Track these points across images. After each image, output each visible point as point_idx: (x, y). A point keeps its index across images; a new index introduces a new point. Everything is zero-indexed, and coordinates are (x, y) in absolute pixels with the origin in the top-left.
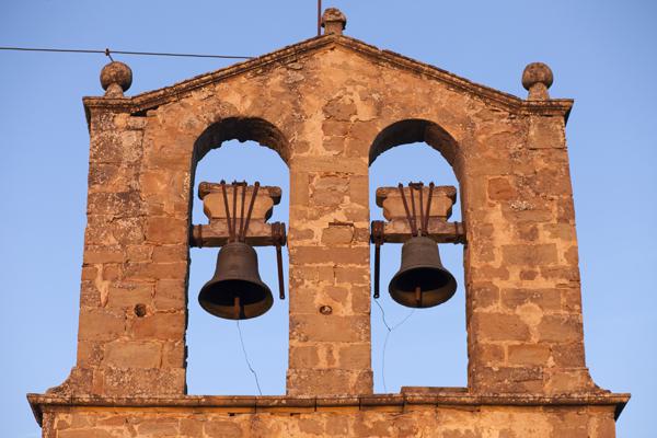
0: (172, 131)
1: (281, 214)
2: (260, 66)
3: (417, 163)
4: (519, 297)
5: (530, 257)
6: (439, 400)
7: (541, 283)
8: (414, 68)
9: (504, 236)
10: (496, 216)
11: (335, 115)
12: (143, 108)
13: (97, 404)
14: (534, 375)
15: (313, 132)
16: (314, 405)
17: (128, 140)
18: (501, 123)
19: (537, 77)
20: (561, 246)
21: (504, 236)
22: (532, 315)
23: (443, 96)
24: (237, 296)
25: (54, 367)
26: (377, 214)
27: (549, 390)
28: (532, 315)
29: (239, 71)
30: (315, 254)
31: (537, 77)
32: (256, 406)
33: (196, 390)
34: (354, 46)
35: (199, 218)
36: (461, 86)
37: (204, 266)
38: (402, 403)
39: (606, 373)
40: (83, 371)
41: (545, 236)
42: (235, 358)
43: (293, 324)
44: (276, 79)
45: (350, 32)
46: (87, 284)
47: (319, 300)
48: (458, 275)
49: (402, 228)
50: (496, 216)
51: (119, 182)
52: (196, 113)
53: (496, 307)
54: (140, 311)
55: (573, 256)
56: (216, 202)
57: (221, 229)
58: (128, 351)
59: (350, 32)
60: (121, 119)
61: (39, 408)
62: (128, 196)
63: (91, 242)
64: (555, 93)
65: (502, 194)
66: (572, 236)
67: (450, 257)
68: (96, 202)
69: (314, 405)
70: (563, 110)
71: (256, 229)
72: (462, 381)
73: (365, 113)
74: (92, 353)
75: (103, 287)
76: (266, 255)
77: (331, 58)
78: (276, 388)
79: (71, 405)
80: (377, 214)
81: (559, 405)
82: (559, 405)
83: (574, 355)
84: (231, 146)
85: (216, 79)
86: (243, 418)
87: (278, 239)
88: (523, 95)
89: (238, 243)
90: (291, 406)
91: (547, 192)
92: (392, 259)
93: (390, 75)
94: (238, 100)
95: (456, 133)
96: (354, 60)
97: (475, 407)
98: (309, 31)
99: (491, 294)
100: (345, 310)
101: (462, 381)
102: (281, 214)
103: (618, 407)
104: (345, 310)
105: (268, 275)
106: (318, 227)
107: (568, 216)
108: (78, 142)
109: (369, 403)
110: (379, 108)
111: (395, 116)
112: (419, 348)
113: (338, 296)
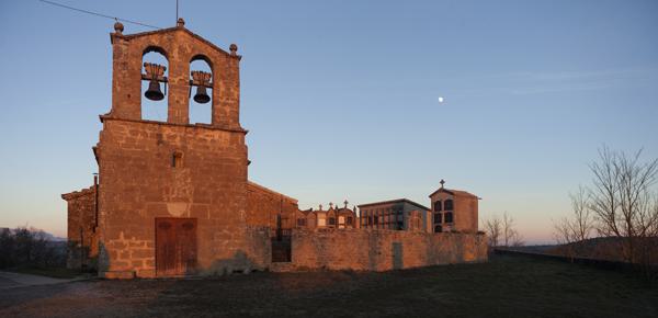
0: (137, 47)
1: (166, 74)
2: (162, 32)
3: (200, 66)
4: (225, 104)
5: (228, 95)
6: (204, 127)
8: (203, 41)
9: (222, 89)
10: (221, 83)
12: (128, 38)
13: (119, 119)
15: (175, 54)
17: (124, 48)
18: (224, 59)
19: (234, 48)
20: (236, 93)
21: (222, 89)
22: (228, 109)
24: (154, 95)
25: (107, 109)
26: (191, 78)
27: (231, 127)
28: (228, 109)
29: (155, 33)
30: (175, 87)
31: (234, 48)
32: (160, 124)
33: (144, 118)
34: (187, 31)
35: (144, 72)
36: (215, 48)
37: (145, 86)
38: (196, 127)
39: (243, 124)
42: (155, 111)
43: (169, 104)
44: (165, 37)
46: (114, 87)
48: (210, 96)
49: (197, 82)
50: (221, 83)
51: (122, 59)
53: (219, 106)
54: (129, 96)
55: (238, 96)
56: (149, 68)
57: (150, 76)
58: (125, 105)
60: (122, 41)
61: (102, 119)
62: (124, 64)
63: (114, 76)
64: (238, 53)
65: (223, 78)
66: (238, 91)
67: (209, 92)
68: (116, 64)
69: (175, 125)
70: (239, 58)
71: (159, 78)
72: (210, 123)
73: (189, 51)
75: (118, 88)
76: (162, 84)
78: (164, 119)
79: (112, 119)
80: (191, 78)
81: (233, 131)
82: (233, 131)
83: (237, 120)
84: (152, 53)
85: (149, 34)
86: (157, 126)
87: (165, 81)
88: (229, 52)
89: (155, 81)
90: (168, 125)
91: (233, 79)
92: (194, 90)
93: (196, 41)
94: (155, 41)
95: (212, 60)
96: (187, 35)
97: (213, 129)
98: (174, 25)
99: (218, 103)
100: (182, 102)
101: (210, 123)
102: (166, 74)
103: (246, 133)
104: (182, 102)
105: (163, 91)
106: (176, 80)
107: (238, 86)
108: (108, 49)
109: (188, 126)
110: (193, 50)
111: (197, 53)
112: (200, 114)
113: (181, 98)
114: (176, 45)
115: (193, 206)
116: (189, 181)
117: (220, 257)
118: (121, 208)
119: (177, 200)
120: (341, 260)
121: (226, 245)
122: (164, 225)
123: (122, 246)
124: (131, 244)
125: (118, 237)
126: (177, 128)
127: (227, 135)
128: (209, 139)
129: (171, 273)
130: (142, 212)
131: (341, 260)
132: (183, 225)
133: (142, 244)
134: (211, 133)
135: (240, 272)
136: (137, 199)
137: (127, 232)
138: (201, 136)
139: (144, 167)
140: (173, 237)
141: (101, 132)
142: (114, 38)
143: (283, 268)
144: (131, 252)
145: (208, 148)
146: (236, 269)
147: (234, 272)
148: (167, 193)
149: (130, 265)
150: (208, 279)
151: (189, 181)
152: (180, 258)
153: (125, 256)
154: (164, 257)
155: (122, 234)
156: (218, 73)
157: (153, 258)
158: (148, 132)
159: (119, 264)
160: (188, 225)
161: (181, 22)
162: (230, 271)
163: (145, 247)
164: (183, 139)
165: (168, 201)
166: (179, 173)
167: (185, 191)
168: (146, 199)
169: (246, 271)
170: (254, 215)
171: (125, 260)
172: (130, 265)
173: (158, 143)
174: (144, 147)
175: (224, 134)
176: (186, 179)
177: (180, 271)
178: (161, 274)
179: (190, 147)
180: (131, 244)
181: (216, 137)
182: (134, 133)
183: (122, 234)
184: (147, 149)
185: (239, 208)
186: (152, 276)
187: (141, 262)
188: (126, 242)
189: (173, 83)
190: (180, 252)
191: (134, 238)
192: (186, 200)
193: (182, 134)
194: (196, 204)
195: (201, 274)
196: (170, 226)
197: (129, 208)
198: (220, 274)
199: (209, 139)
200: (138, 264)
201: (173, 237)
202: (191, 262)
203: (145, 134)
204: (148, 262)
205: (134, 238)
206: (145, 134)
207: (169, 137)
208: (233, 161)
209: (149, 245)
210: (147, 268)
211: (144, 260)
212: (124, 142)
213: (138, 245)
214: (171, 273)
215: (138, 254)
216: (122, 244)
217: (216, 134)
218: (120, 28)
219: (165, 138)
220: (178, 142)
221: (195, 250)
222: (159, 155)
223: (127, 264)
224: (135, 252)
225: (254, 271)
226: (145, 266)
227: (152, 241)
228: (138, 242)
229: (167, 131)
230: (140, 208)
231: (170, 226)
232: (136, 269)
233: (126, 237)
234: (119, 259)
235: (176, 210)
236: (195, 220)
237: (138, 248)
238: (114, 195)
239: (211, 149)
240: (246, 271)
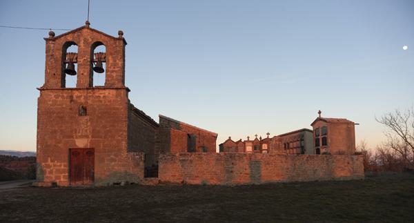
0: (59, 44)
2: (73, 32)
4: (113, 71)
7: (116, 69)
10: (110, 58)
11: (85, 40)
14: (114, 84)
15: (82, 44)
16: (80, 89)
17: (52, 45)
18: (112, 42)
19: (121, 33)
21: (111, 62)
23: (103, 37)
25: (41, 83)
27: (116, 86)
29: (69, 33)
31: (121, 33)
40: (45, 85)
41: (117, 61)
42: (71, 81)
45: (90, 26)
46: (46, 70)
47: (82, 72)
50: (110, 58)
51: (50, 53)
52: (63, 41)
59: (90, 26)
68: (47, 56)
69: (80, 89)
72: (103, 85)
73: (90, 40)
74: (47, 81)
77: (85, 30)
79: (43, 90)
81: (117, 89)
82: (117, 89)
85: (66, 34)
93: (95, 33)
94: (70, 38)
96: (89, 31)
105: (76, 70)
106: (82, 60)
110: (93, 39)
114: (82, 38)
116: (89, 124)
118: (49, 143)
119: (82, 137)
120: (196, 177)
121: (117, 165)
122: (74, 153)
123: (49, 166)
124: (55, 166)
125: (47, 161)
126: (81, 91)
127: (114, 92)
128: (102, 96)
129: (79, 183)
131: (196, 177)
132: (87, 153)
133: (61, 165)
134: (103, 91)
136: (58, 137)
137: (52, 158)
138: (97, 95)
139: (61, 118)
140: (80, 161)
141: (39, 99)
142: (47, 40)
143: (152, 181)
145: (101, 101)
148: (76, 132)
149: (54, 179)
150: (102, 189)
151: (89, 124)
152: (85, 174)
153: (51, 172)
154: (75, 173)
155: (49, 160)
156: (106, 52)
157: (67, 174)
158: (65, 95)
159: (47, 177)
160: (90, 152)
161: (88, 23)
162: (111, 183)
163: (62, 167)
164: (86, 98)
165: (76, 138)
166: (84, 119)
167: (86, 131)
168: (63, 137)
169: (123, 184)
171: (51, 175)
173: (71, 102)
174: (62, 105)
175: (111, 91)
176: (87, 122)
177: (87, 183)
178: (73, 184)
179: (90, 102)
181: (107, 94)
182: (57, 97)
183: (49, 160)
184: (64, 106)
185: (122, 140)
186: (66, 185)
188: (51, 164)
189: (84, 59)
192: (87, 137)
193: (85, 94)
196: (79, 154)
197: (54, 143)
199: (102, 96)
200: (58, 178)
201: (80, 161)
202: (93, 178)
203: (63, 97)
206: (63, 97)
207: (77, 97)
208: (118, 109)
209: (65, 166)
210: (63, 180)
211: (62, 175)
212: (51, 103)
215: (58, 171)
216: (49, 165)
217: (107, 92)
218: (52, 34)
219: (75, 98)
220: (82, 100)
222: (71, 109)
223: (52, 178)
224: (57, 169)
226: (62, 180)
228: (59, 164)
229: (76, 93)
230: (59, 143)
231: (79, 154)
232: (58, 181)
233: (52, 161)
234: (47, 175)
235: (81, 143)
236: (93, 149)
237: (58, 168)
238: (45, 135)
239: (103, 103)
240: (123, 184)
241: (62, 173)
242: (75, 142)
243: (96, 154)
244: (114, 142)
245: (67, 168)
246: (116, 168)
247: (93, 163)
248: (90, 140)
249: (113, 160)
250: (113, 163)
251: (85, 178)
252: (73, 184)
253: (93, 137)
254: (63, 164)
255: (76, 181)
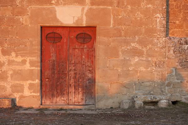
115: (90, 9)
117: (126, 81)
122: (51, 35)
124: (10, 62)
129: (60, 102)
130: (24, 19)
132: (77, 37)
133: (24, 62)
135: (155, 103)
144: (11, 72)
146: (149, 99)
147: (145, 103)
150: (110, 115)
152: (72, 81)
154: (52, 80)
157: (37, 81)
160: (85, 35)
162: (139, 102)
163: (27, 66)
169: (163, 103)
170: (180, 26)
172: (9, 91)
177: (74, 100)
178: (47, 103)
180: (10, 62)
185: (155, 11)
186: (36, 104)
187: (22, 86)
190: (72, 73)
191: (13, 54)
194: (94, 7)
195: (102, 104)
198: (126, 106)
200: (18, 88)
202: (89, 88)
204: (31, 86)
205: (13, 54)
209: (32, 63)
213: (18, 64)
214: (60, 102)
215: (18, 74)
221: (93, 71)
225: (174, 103)
227: (36, 58)
228: (19, 59)
232: (17, 96)
235: (68, 16)
236: (93, 29)
237: (18, 68)
240: (163, 103)
241: (25, 79)
242: (53, 12)
243: (99, 38)
244: (139, 15)
245: (37, 69)
246: (142, 69)
247: (91, 56)
248: (86, 8)
249: (136, 52)
250: (137, 59)
251: (72, 90)
252: (47, 103)
253: (92, 4)
254: (28, 59)
255: (53, 96)
